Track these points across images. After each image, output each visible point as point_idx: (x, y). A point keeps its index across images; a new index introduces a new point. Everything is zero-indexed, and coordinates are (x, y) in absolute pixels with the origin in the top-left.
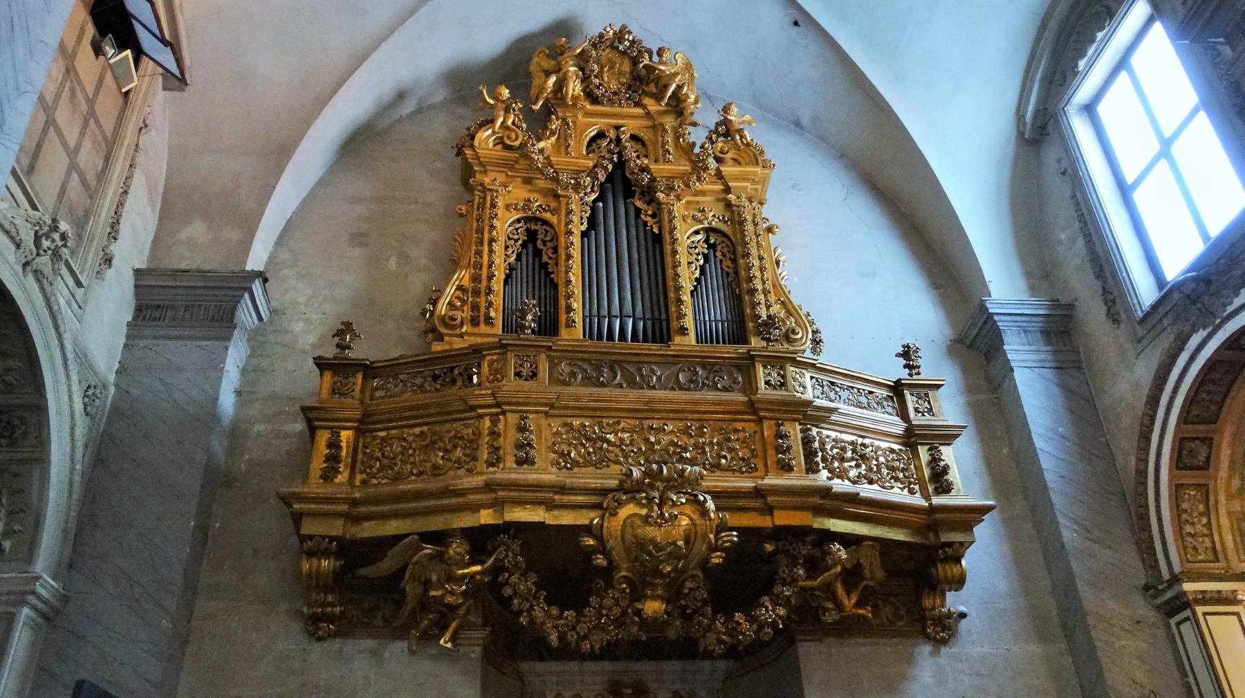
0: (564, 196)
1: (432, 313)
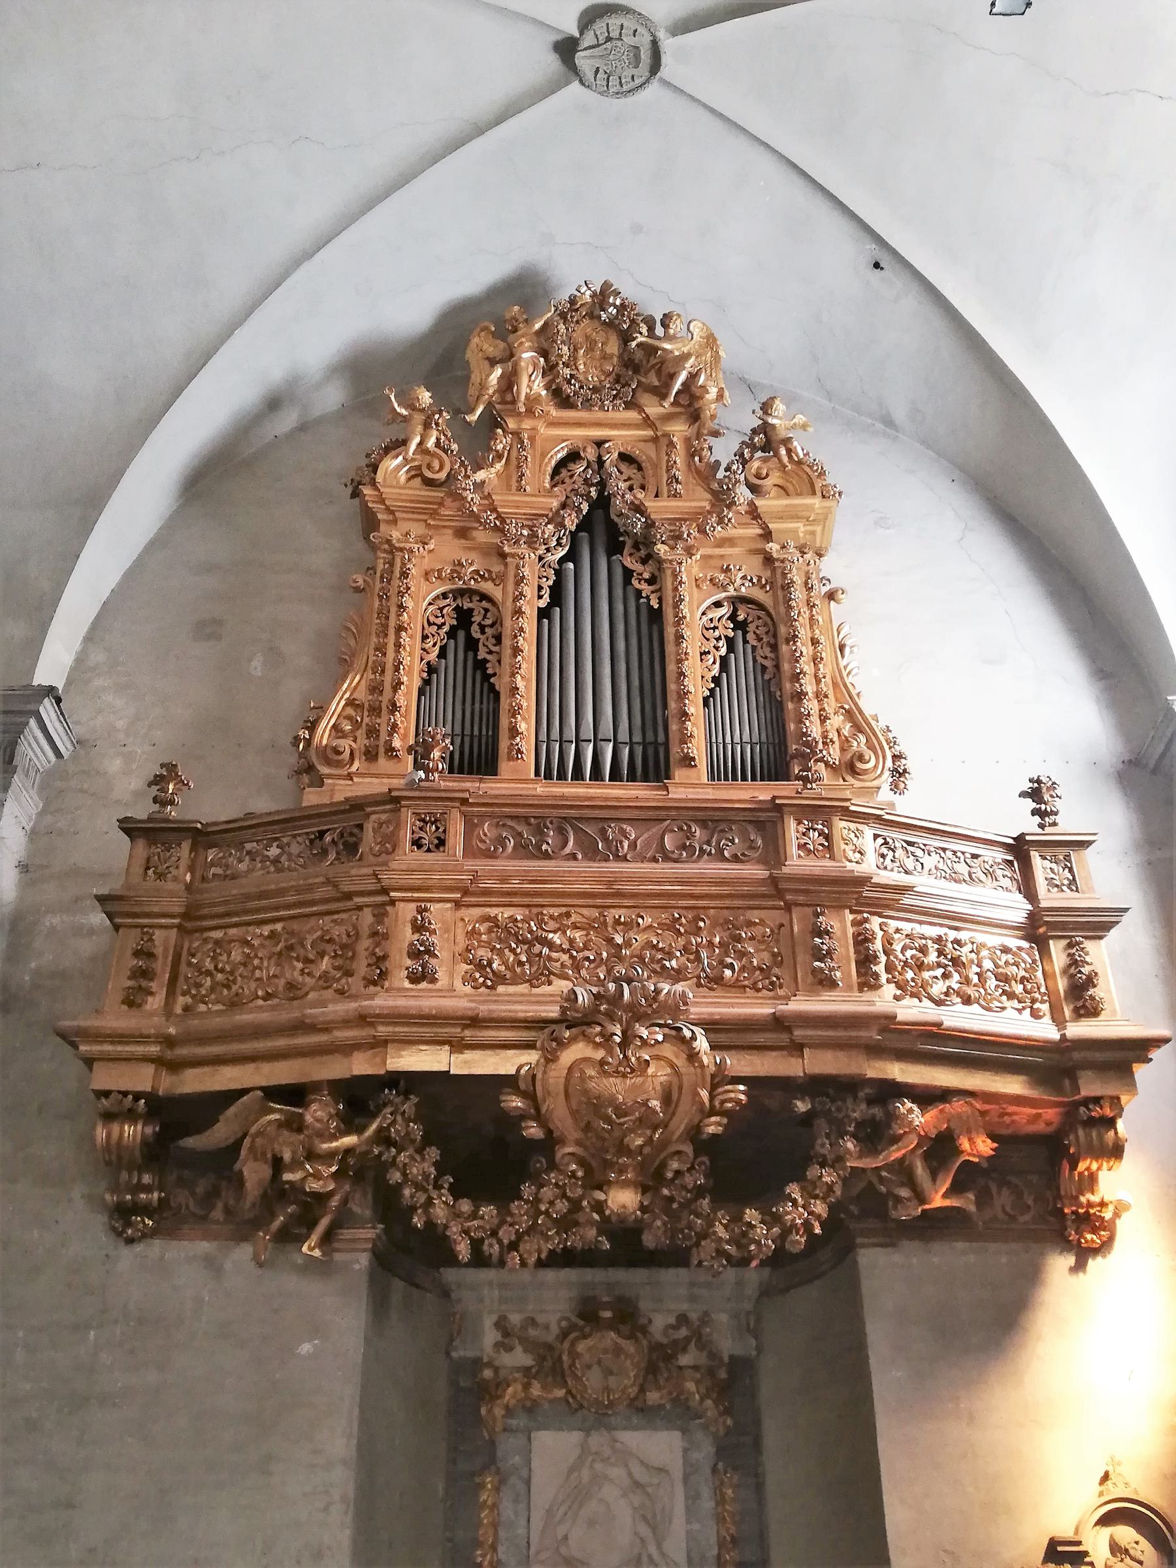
0: (513, 555)
1: (308, 742)
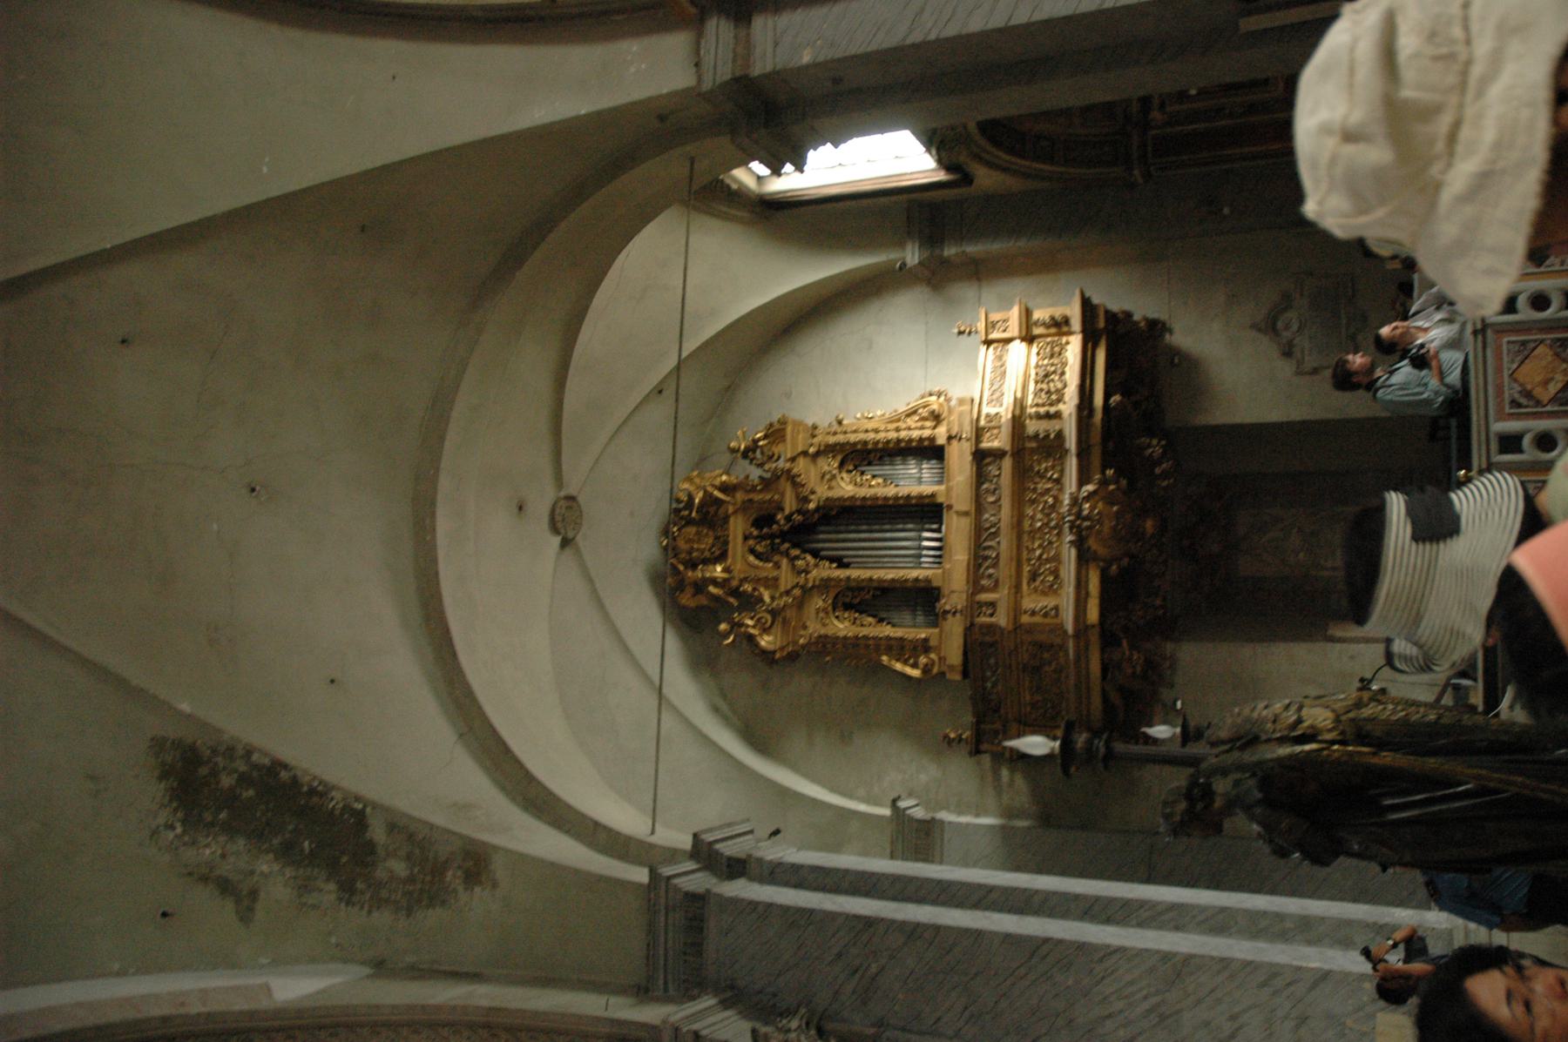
0: (814, 581)
